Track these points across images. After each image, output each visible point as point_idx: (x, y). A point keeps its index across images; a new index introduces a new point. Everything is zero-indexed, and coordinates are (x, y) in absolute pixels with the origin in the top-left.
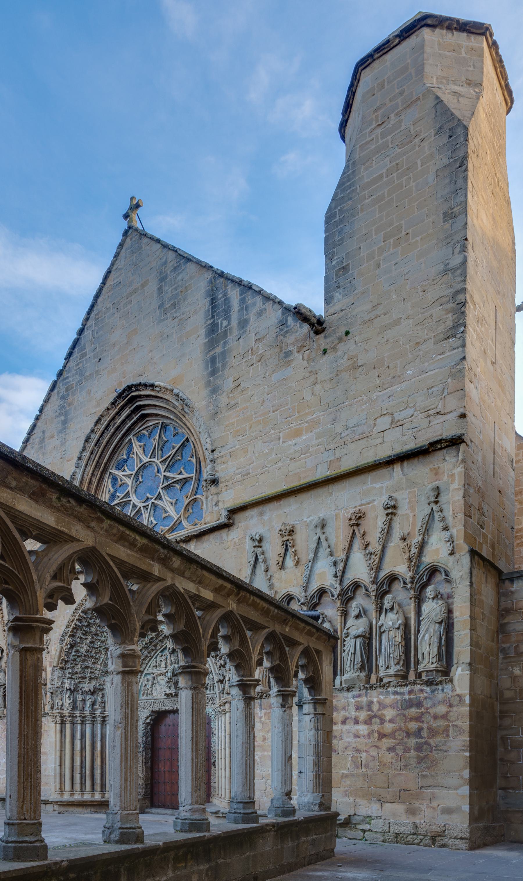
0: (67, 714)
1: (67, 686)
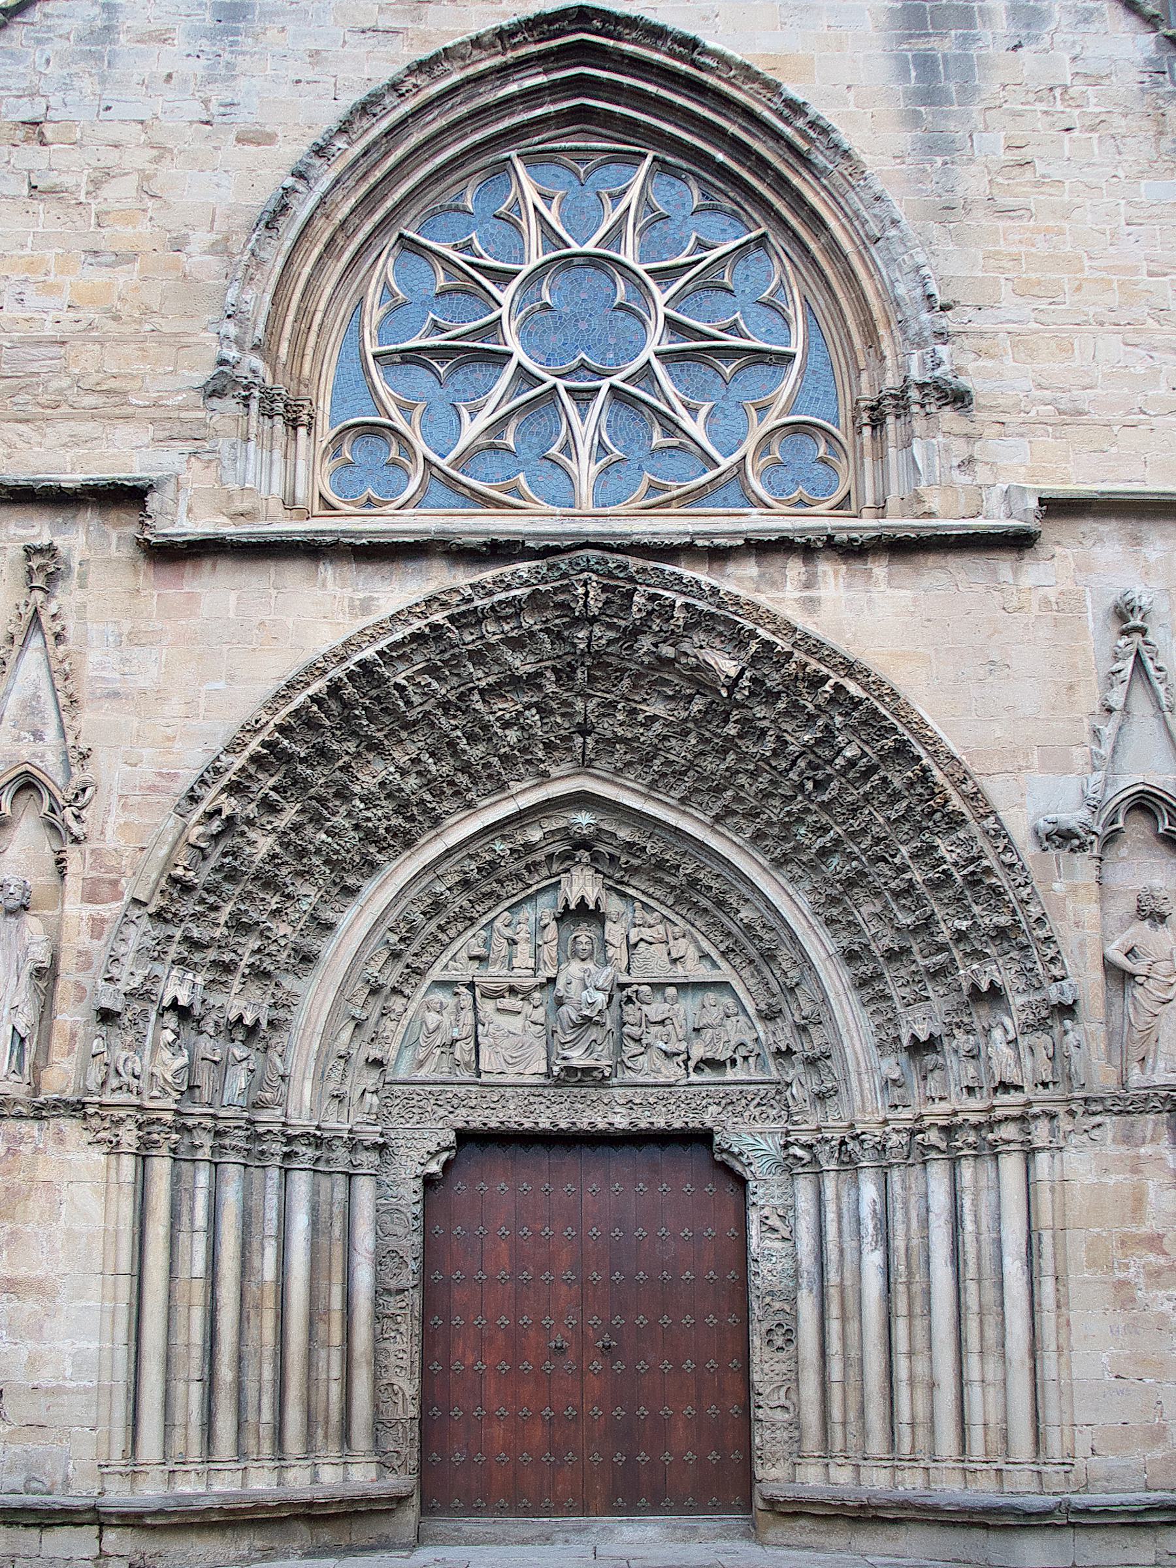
1: (178, 987)
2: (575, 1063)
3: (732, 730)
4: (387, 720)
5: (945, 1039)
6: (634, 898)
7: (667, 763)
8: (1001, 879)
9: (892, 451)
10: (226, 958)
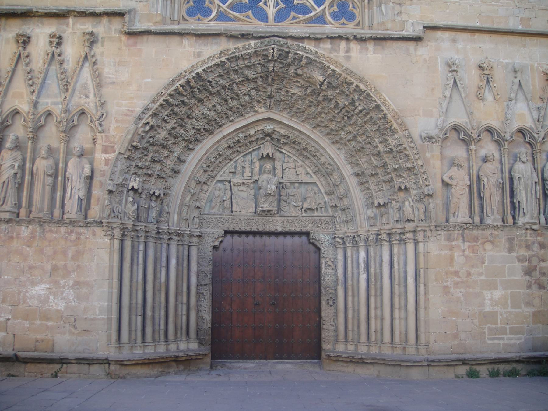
0: (131, 227)
2: (265, 209)
3: (320, 98)
4: (204, 92)
5: (389, 204)
6: (284, 153)
7: (298, 109)
8: (409, 152)
9: (375, 8)
10: (150, 172)
